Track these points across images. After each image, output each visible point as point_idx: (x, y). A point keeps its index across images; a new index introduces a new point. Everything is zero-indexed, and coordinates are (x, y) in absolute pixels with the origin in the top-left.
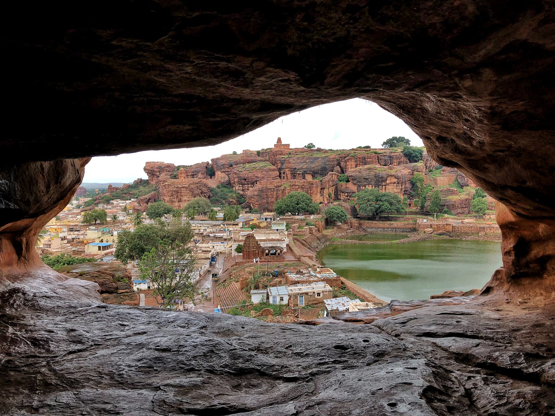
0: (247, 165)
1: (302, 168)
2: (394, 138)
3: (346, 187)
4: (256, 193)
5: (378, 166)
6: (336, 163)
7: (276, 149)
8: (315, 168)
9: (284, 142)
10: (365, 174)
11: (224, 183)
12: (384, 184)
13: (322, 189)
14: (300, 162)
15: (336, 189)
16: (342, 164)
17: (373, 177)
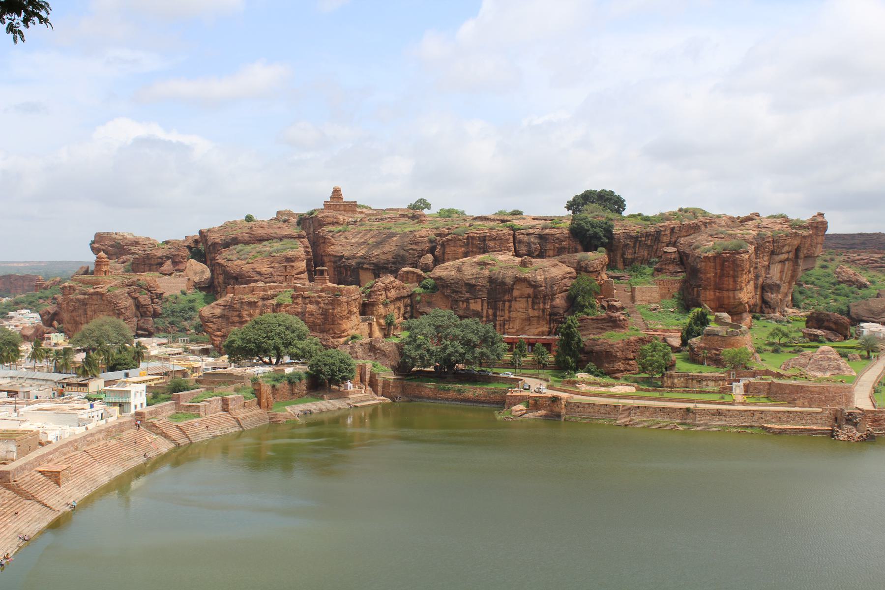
1: (354, 257)
4: (218, 311)
6: (426, 246)
8: (382, 257)
9: (347, 197)
12: (506, 298)
17: (485, 282)
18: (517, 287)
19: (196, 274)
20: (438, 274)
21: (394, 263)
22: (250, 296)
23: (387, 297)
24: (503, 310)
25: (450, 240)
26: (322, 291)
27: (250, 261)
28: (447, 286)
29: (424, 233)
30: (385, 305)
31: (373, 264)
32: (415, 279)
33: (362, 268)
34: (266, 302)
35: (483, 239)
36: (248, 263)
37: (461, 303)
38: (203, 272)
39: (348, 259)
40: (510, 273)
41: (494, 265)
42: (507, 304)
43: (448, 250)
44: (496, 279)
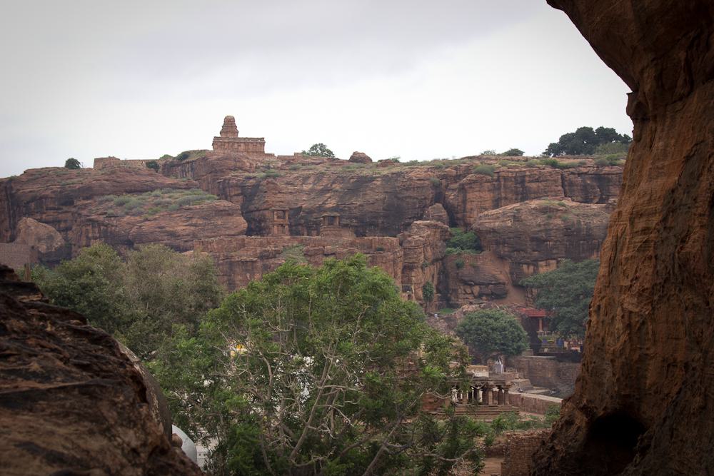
0: (134, 199)
1: (321, 209)
2: (584, 133)
5: (568, 202)
6: (430, 193)
9: (244, 132)
10: (535, 223)
11: (48, 254)
13: (408, 268)
14: (312, 190)
15: (444, 273)
16: (451, 196)
19: (39, 240)
20: (487, 225)
22: (240, 252)
25: (474, 182)
27: (150, 217)
29: (423, 175)
31: (356, 218)
36: (147, 220)
37: (525, 267)
38: (51, 238)
39: (310, 212)
41: (566, 212)
43: (470, 195)
44: (579, 230)
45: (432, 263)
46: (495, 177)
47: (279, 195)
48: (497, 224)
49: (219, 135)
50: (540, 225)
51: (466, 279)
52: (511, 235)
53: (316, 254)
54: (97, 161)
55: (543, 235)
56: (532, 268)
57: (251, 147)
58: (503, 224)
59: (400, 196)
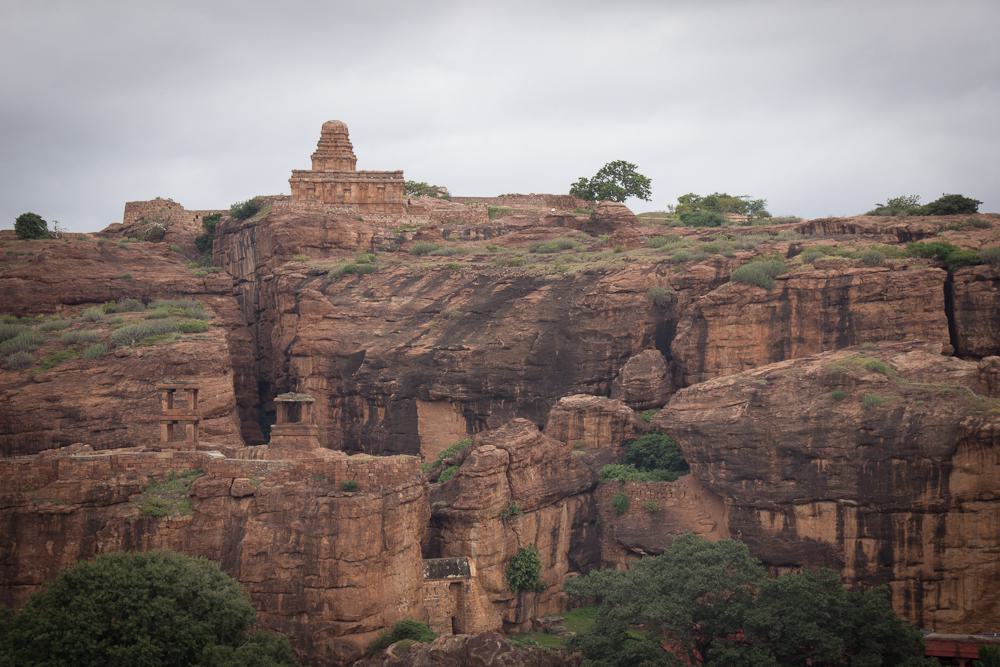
1: (398, 358)
3: (657, 515)
7: (300, 208)
9: (369, 157)
10: (794, 409)
12: (926, 498)
14: (406, 310)
18: (965, 460)
21: (529, 379)
23: (512, 494)
24: (915, 542)
25: (726, 302)
26: (296, 473)
28: (718, 459)
30: (508, 517)
31: (464, 382)
32: (606, 432)
33: (428, 399)
34: (101, 513)
35: (839, 296)
37: (765, 516)
39: (378, 366)
40: (939, 412)
42: (929, 521)
43: (716, 333)
45: (553, 499)
46: (778, 291)
47: (325, 324)
48: (709, 413)
49: (307, 166)
50: (806, 419)
51: (628, 541)
52: (736, 442)
53: (212, 496)
54: (131, 207)
55: (809, 442)
56: (780, 519)
57: (372, 192)
58: (721, 414)
59: (572, 330)
